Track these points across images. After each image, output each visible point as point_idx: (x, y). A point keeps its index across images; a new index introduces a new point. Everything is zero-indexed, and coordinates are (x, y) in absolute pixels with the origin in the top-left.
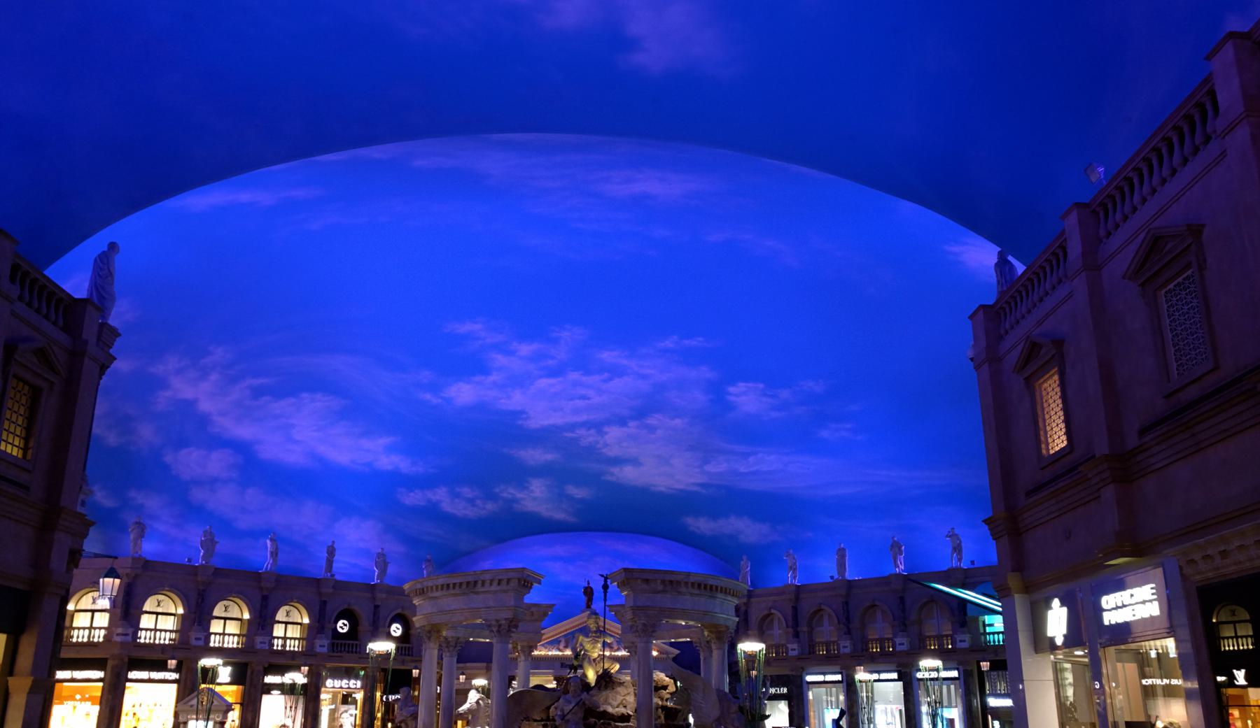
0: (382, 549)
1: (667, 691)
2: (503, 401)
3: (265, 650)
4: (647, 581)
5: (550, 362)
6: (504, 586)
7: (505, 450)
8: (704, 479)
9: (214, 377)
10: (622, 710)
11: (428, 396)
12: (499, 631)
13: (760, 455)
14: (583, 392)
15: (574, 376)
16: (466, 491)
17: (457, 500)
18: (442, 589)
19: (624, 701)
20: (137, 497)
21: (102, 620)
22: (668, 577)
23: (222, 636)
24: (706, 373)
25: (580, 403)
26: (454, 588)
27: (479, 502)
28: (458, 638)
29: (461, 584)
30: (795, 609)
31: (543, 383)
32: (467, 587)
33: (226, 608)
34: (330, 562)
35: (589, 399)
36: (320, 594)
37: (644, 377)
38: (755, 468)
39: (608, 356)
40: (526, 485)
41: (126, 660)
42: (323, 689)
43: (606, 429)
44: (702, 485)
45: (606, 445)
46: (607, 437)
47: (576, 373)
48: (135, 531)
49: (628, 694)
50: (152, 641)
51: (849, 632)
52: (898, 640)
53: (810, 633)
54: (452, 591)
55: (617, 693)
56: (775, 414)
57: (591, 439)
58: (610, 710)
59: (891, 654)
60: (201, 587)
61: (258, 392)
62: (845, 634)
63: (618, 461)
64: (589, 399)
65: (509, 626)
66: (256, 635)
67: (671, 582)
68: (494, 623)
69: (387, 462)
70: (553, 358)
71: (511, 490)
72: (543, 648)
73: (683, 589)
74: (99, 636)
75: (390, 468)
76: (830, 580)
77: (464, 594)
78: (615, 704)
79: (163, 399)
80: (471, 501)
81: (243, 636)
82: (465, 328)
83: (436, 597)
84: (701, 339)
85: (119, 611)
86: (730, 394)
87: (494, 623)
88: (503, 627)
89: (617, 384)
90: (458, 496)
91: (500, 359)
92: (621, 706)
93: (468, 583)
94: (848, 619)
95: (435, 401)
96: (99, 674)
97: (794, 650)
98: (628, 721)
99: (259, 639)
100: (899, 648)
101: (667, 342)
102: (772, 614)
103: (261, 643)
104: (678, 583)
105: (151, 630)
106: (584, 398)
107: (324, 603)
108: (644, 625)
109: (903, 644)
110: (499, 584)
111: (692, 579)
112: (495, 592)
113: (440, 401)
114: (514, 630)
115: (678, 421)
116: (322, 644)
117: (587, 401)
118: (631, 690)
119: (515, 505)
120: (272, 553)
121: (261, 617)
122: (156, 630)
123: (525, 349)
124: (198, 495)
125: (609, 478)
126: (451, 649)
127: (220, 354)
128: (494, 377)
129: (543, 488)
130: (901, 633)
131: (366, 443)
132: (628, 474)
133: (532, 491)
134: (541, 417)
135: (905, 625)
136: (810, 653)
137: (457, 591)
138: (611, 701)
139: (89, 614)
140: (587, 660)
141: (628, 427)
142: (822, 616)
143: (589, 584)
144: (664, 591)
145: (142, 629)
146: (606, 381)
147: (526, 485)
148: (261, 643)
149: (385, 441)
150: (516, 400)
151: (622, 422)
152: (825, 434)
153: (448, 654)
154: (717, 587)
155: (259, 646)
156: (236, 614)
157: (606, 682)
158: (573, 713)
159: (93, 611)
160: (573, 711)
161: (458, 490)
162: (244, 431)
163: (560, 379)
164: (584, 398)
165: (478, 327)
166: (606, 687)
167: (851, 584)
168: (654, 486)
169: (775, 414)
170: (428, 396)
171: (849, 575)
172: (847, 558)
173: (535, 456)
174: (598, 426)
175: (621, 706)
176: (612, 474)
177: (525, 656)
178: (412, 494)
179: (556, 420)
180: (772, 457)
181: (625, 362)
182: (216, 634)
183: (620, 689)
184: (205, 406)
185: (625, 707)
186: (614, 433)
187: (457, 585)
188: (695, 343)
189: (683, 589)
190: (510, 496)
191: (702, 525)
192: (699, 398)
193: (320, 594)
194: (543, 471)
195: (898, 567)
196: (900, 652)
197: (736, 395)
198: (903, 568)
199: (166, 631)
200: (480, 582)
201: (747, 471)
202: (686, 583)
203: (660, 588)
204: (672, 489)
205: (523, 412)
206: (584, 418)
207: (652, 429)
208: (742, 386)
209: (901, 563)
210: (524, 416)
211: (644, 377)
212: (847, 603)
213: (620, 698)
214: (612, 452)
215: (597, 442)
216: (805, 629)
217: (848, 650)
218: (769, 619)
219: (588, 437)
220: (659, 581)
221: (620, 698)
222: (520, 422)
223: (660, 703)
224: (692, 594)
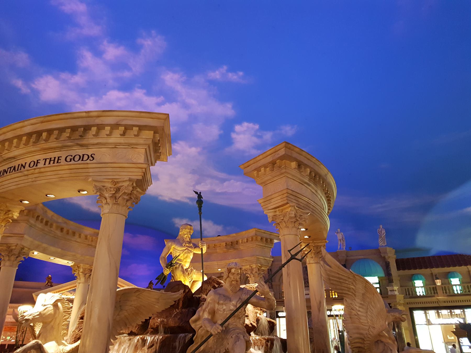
2: (78, 105)
5: (127, 74)
12: (114, 197)
13: (232, 181)
29: (61, 130)
68: (109, 185)
70: (129, 69)
72: (69, 294)
84: (241, 73)
86: (234, 131)
87: (109, 185)
93: (74, 129)
95: (25, 90)
110: (124, 134)
112: (116, 146)
126: (13, 258)
128: (78, 79)
140: (180, 268)
146: (159, 104)
153: (8, 263)
163: (127, 94)
170: (19, 83)
180: (238, 183)
181: (179, 88)
187: (56, 132)
188: (235, 77)
201: (220, 191)
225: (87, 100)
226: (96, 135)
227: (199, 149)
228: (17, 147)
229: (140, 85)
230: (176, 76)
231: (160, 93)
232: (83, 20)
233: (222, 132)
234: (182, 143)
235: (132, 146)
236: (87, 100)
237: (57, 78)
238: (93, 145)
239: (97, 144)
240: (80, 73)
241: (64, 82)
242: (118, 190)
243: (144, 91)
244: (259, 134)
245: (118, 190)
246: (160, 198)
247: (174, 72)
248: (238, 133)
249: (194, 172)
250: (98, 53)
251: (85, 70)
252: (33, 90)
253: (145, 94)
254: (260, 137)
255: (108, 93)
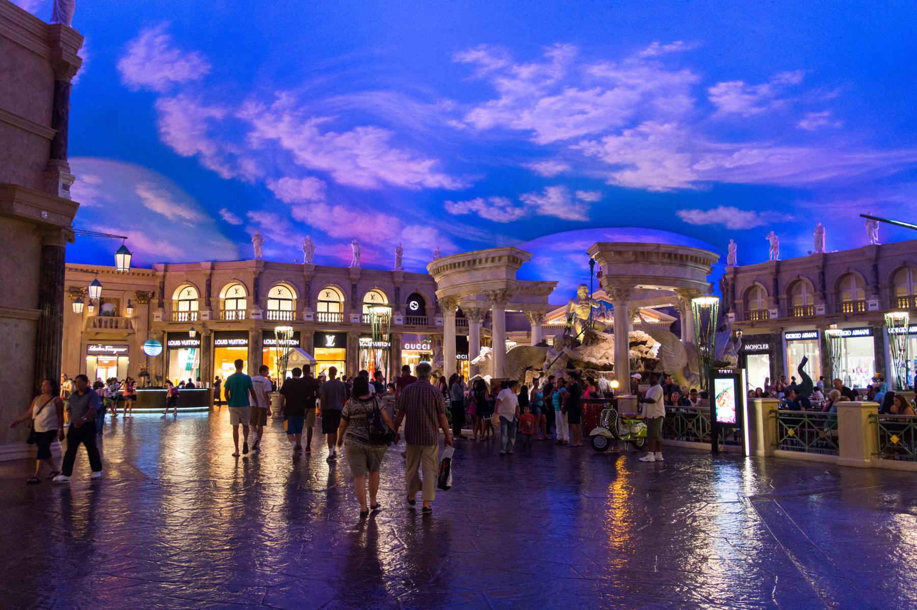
0: (438, 248)
1: (647, 345)
2: (514, 122)
3: (357, 323)
4: (620, 253)
5: (549, 82)
6: (497, 263)
7: (524, 165)
8: (694, 177)
9: (287, 118)
10: (604, 361)
11: (454, 123)
12: (495, 299)
13: (744, 151)
14: (580, 107)
15: (571, 93)
16: (498, 201)
17: (491, 208)
18: (451, 268)
19: (606, 354)
20: (255, 216)
21: (243, 305)
22: (639, 249)
23: (326, 314)
24: (687, 77)
25: (580, 118)
26: (459, 266)
27: (508, 209)
28: (479, 309)
29: (464, 262)
30: (776, 281)
31: (546, 102)
32: (468, 265)
33: (328, 294)
34: (399, 260)
35: (586, 113)
36: (394, 283)
37: (632, 87)
38: (741, 163)
39: (598, 70)
40: (544, 193)
41: (260, 331)
42: (403, 351)
43: (605, 139)
44: (694, 183)
45: (606, 154)
46: (606, 146)
47: (572, 90)
48: (256, 241)
49: (610, 348)
50: (291, 319)
51: (824, 297)
52: (870, 302)
53: (790, 299)
54: (457, 269)
55: (600, 347)
56: (756, 111)
57: (593, 150)
58: (594, 361)
59: (862, 314)
60: (307, 280)
61: (324, 129)
62: (821, 299)
63: (618, 167)
64: (586, 113)
65: (504, 295)
66: (350, 313)
67: (643, 253)
68: (491, 293)
69: (435, 181)
70: (550, 77)
71: (534, 198)
73: (654, 259)
74: (242, 315)
75: (436, 185)
76: (808, 255)
77: (467, 271)
78: (599, 356)
79: (254, 140)
80: (502, 209)
81: (342, 313)
82: (472, 56)
83: (447, 275)
84: (680, 43)
85: (251, 298)
87: (491, 293)
88: (498, 296)
89: (610, 97)
90: (491, 205)
91: (505, 84)
92: (604, 358)
93: (469, 262)
94: (824, 286)
95: (461, 126)
96: (245, 342)
97: (775, 314)
98: (611, 370)
99: (352, 316)
100: (870, 309)
101: (649, 50)
102: (757, 286)
103: (354, 318)
104: (649, 253)
105: (276, 311)
106: (583, 112)
107: (397, 290)
108: (619, 290)
109: (875, 305)
111: (662, 250)
112: (490, 268)
113: (464, 126)
114: (509, 298)
115: (667, 127)
116: (398, 318)
117: (585, 116)
118: (612, 345)
119: (538, 210)
120: (356, 254)
121: (352, 300)
122: (279, 310)
123: (526, 71)
124: (299, 213)
125: (612, 182)
127: (284, 98)
128: (504, 101)
129: (559, 195)
130: (873, 296)
131: (414, 166)
132: (628, 179)
133: (550, 198)
134: (547, 135)
135: (877, 288)
136: (789, 316)
137: (462, 269)
138: (595, 354)
139: (235, 300)
141: (624, 136)
142: (800, 285)
143: (601, 269)
144: (636, 261)
145: (269, 310)
147: (544, 193)
148: (354, 318)
149: (428, 163)
150: (525, 120)
151: (618, 132)
152: (804, 124)
154: (687, 256)
155: (352, 321)
156: (336, 298)
157: (592, 338)
158: (557, 363)
159: (237, 299)
160: (557, 361)
161: (491, 200)
162: (321, 162)
163: (559, 97)
164: (583, 112)
165: (481, 54)
166: (592, 343)
167: (825, 255)
168: (649, 186)
169: (756, 111)
170: (454, 123)
171: (824, 250)
172: (824, 235)
173: (548, 168)
174: (597, 138)
175: (604, 358)
176: (614, 179)
177: (536, 322)
178: (456, 205)
179: (562, 135)
180: (755, 152)
181: (612, 74)
182: (322, 313)
183: (602, 344)
184: (287, 143)
185: (607, 358)
186: (612, 142)
188: (675, 47)
189: (654, 259)
190: (533, 203)
191: (695, 217)
192: (684, 102)
193: (394, 283)
194: (558, 180)
195: (873, 239)
196: (872, 312)
197: (719, 96)
198: (877, 239)
199: (286, 311)
200: (478, 261)
201: (732, 166)
202: (658, 253)
203: (632, 258)
204: (666, 188)
205: (533, 131)
206: (584, 131)
207: (645, 136)
208: (722, 86)
209: (875, 236)
210: (534, 134)
211: (632, 87)
212: (823, 273)
213: (602, 352)
214: (612, 160)
215: (599, 152)
216: (785, 296)
217: (823, 312)
218: (754, 290)
219: (590, 148)
220: (631, 253)
221: (602, 352)
222: (532, 140)
223: (640, 355)
224: (663, 263)
225: (521, 115)
226: (480, 263)
227: (674, 124)
228: (447, 269)
229: (568, 86)
230: (603, 67)
231: (594, 85)
232: (487, 60)
233: (694, 100)
234: (649, 123)
235: (498, 267)
236: (521, 115)
237: (484, 108)
238: (480, 268)
239: (482, 268)
240: (504, 97)
241: (492, 107)
242: (496, 295)
243: (576, 89)
244: (749, 90)
245: (496, 295)
246: (650, 189)
247: (600, 64)
248: (719, 96)
249: (681, 150)
250: (514, 77)
251: (507, 93)
252: (468, 124)
253: (578, 91)
254: (753, 93)
255: (540, 103)
